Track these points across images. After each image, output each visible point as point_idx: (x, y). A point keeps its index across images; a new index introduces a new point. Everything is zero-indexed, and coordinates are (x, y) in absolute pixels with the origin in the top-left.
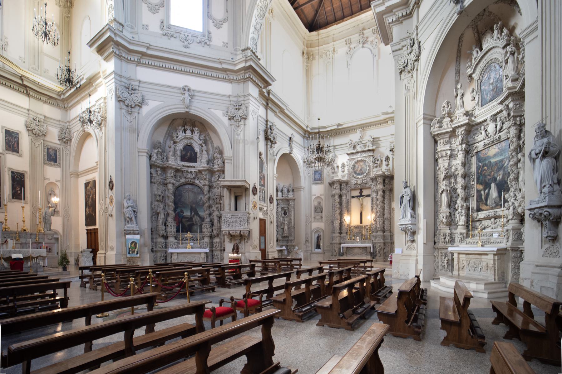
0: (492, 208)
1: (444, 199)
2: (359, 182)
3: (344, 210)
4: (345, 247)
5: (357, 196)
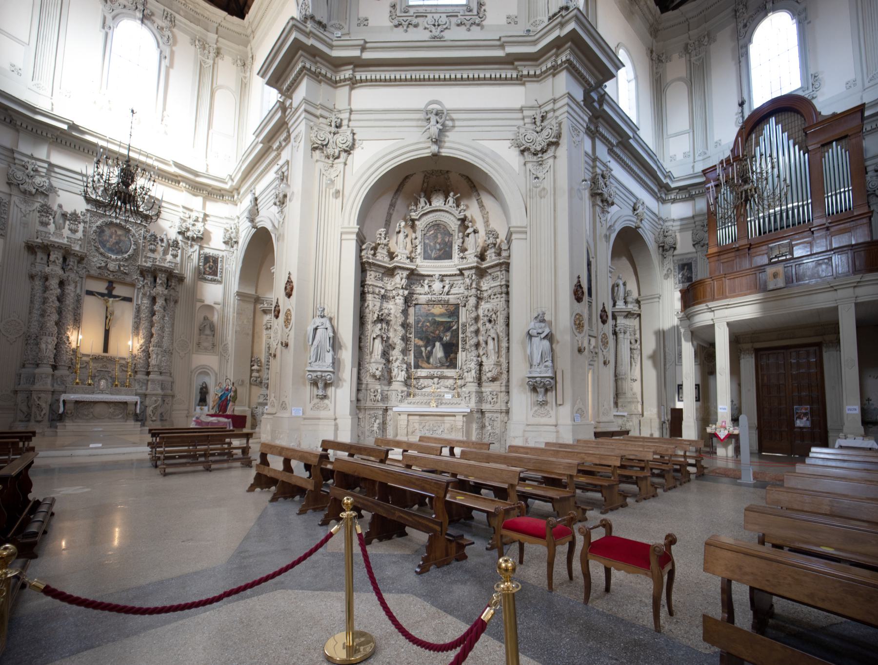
0: (437, 368)
1: (378, 347)
2: (112, 266)
3: (70, 317)
4: (70, 402)
5: (102, 295)
